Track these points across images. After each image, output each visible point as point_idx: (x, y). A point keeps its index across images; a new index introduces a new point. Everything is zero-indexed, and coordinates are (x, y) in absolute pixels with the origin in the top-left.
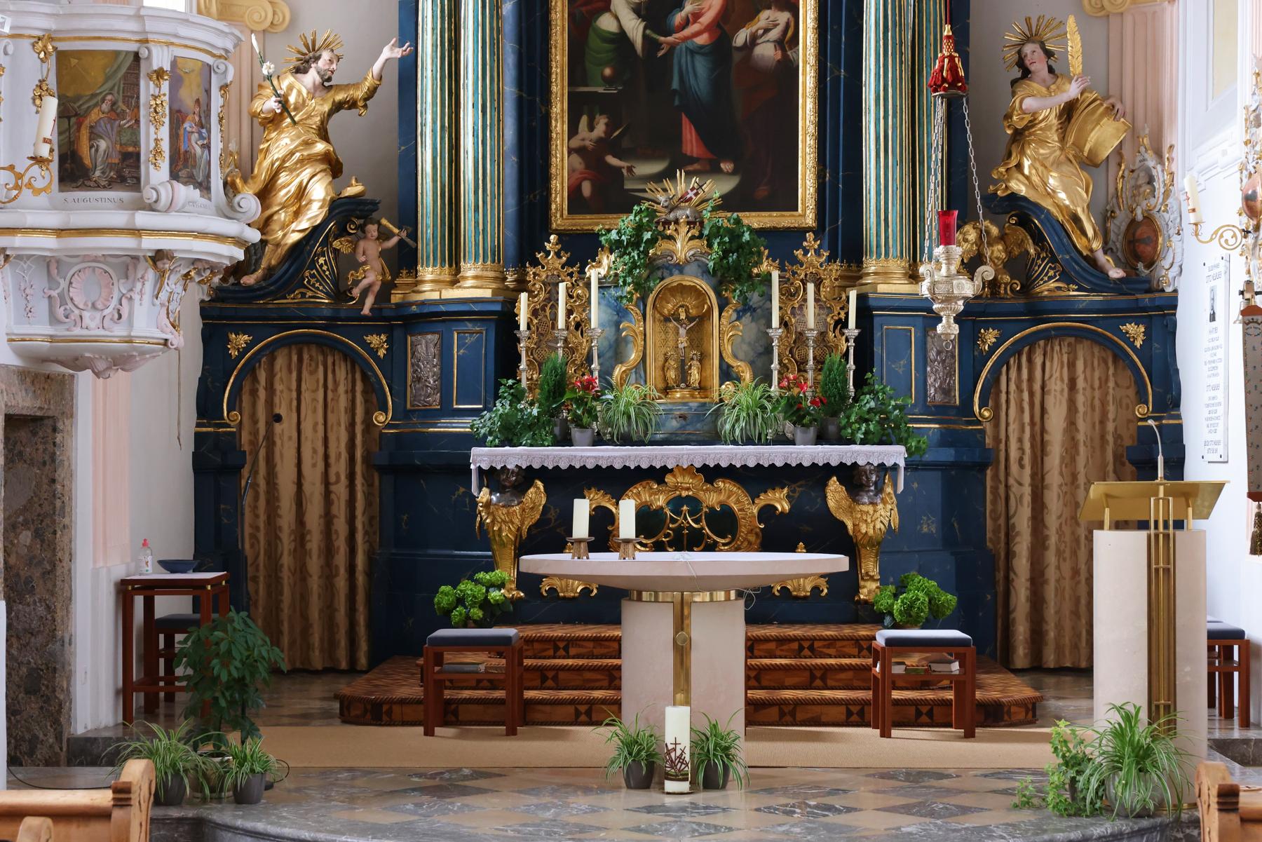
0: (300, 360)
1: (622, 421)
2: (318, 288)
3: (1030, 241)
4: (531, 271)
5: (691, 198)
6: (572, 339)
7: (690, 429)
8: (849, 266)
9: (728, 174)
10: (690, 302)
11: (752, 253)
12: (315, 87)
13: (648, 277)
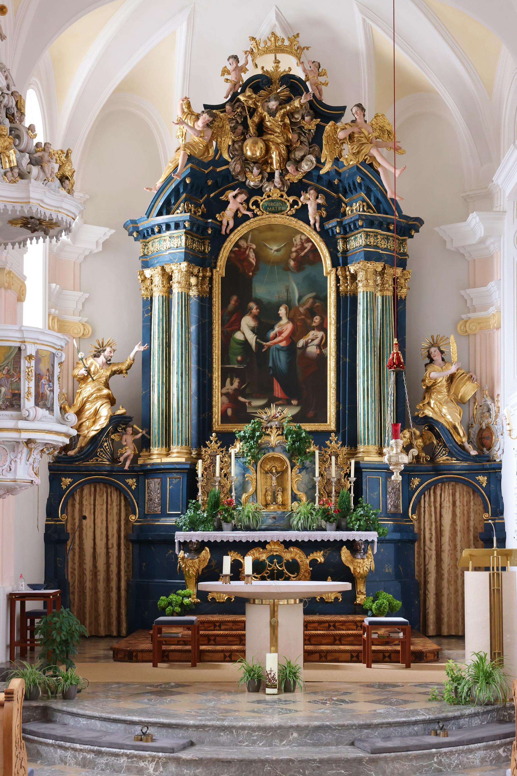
0: (95, 490)
1: (246, 520)
2: (104, 457)
3: (434, 438)
4: (203, 449)
5: (278, 417)
6: (222, 481)
7: (277, 524)
8: (351, 449)
9: (295, 405)
10: (278, 464)
11: (306, 442)
12: (103, 364)
13: (258, 453)
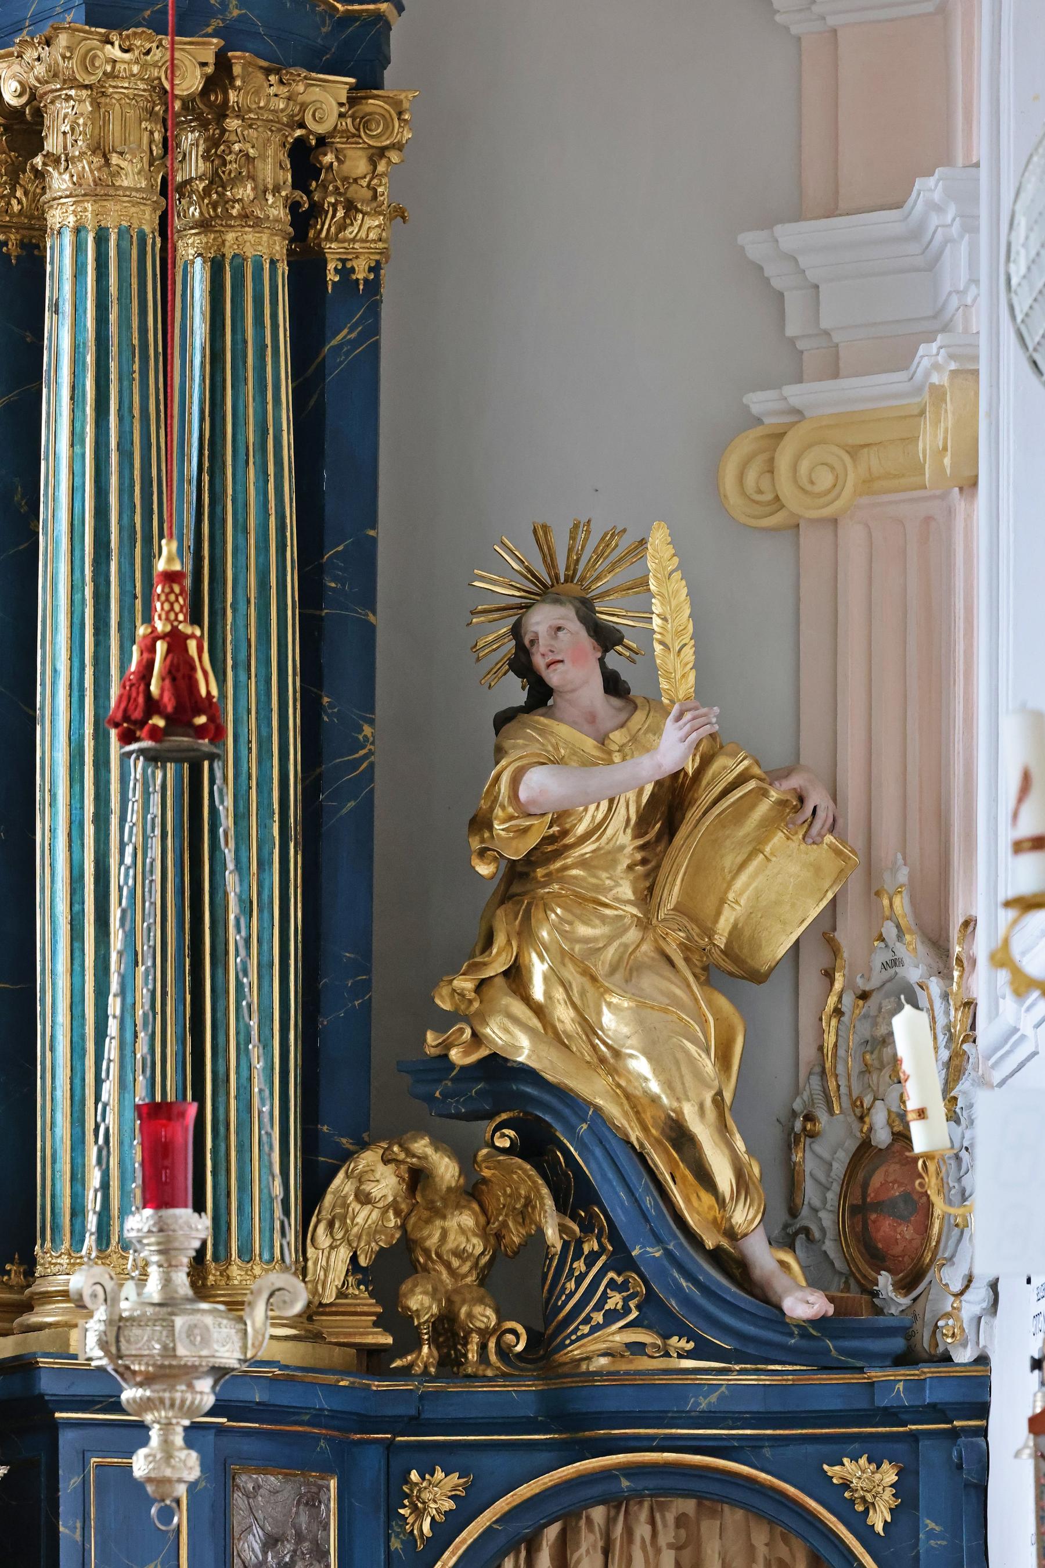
3: (549, 1203)
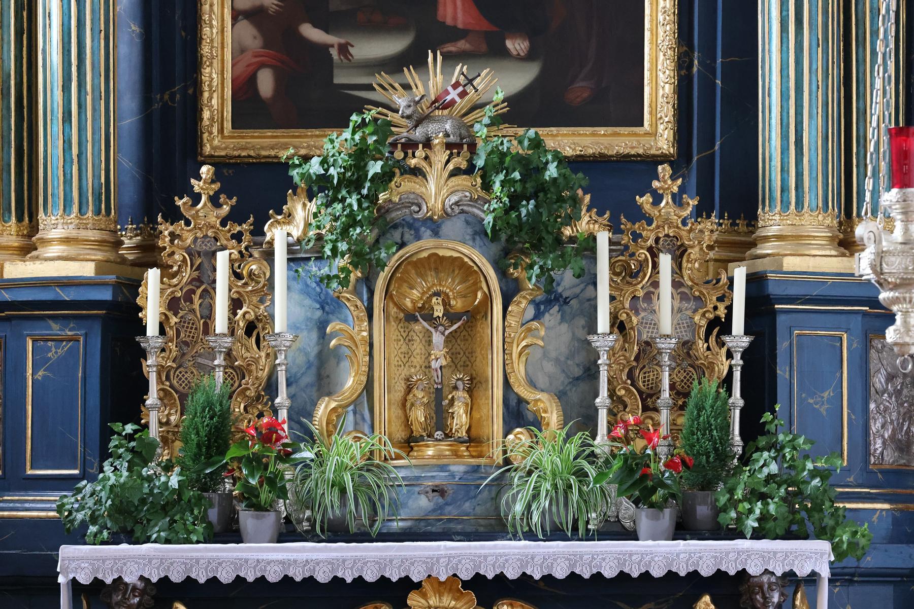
1: (331, 498)
4: (166, 229)
5: (453, 102)
6: (239, 351)
7: (451, 512)
8: (734, 224)
9: (519, 58)
10: (452, 286)
11: (561, 200)
13: (377, 241)
